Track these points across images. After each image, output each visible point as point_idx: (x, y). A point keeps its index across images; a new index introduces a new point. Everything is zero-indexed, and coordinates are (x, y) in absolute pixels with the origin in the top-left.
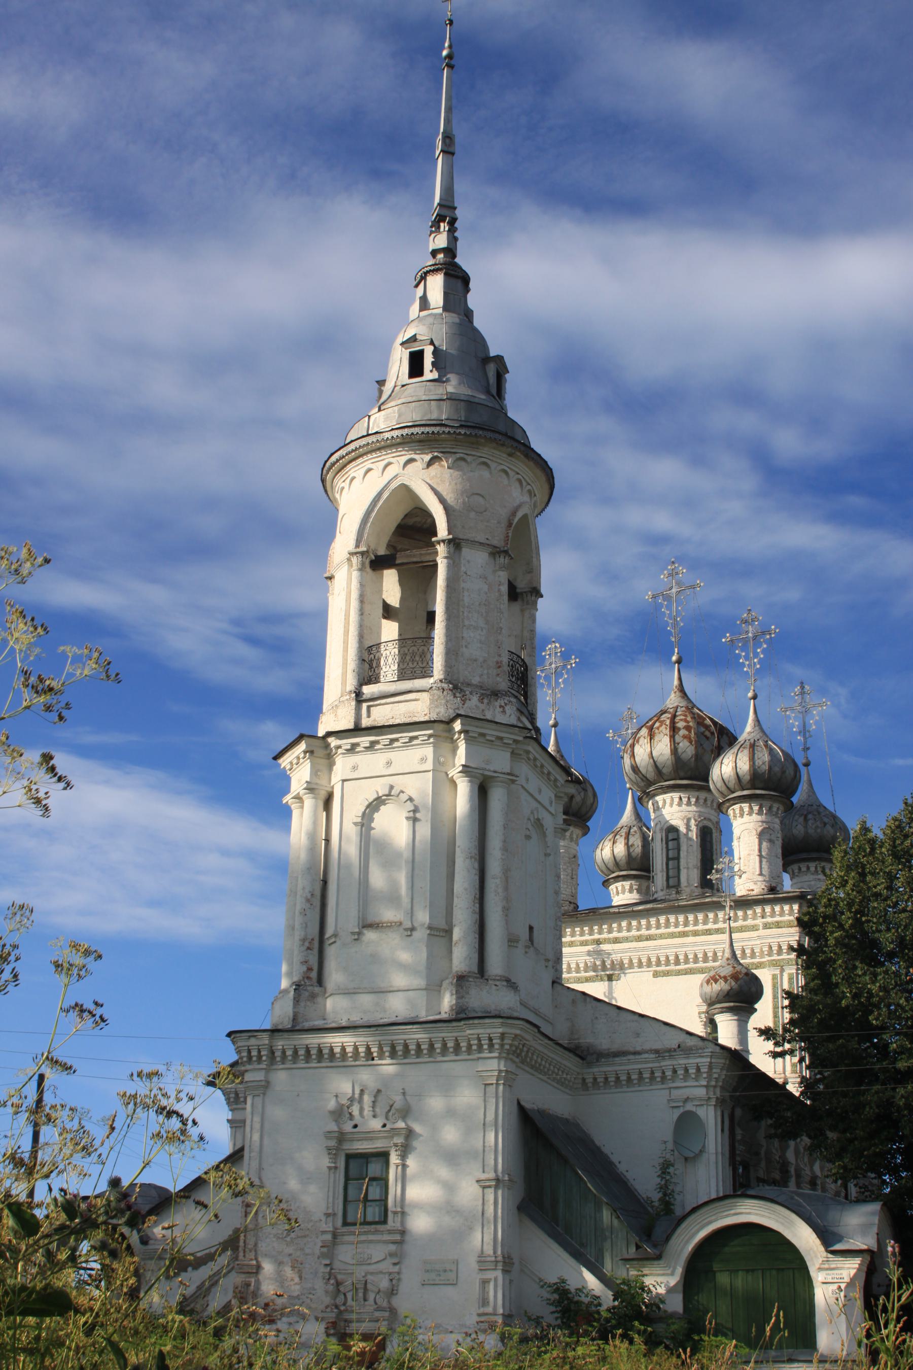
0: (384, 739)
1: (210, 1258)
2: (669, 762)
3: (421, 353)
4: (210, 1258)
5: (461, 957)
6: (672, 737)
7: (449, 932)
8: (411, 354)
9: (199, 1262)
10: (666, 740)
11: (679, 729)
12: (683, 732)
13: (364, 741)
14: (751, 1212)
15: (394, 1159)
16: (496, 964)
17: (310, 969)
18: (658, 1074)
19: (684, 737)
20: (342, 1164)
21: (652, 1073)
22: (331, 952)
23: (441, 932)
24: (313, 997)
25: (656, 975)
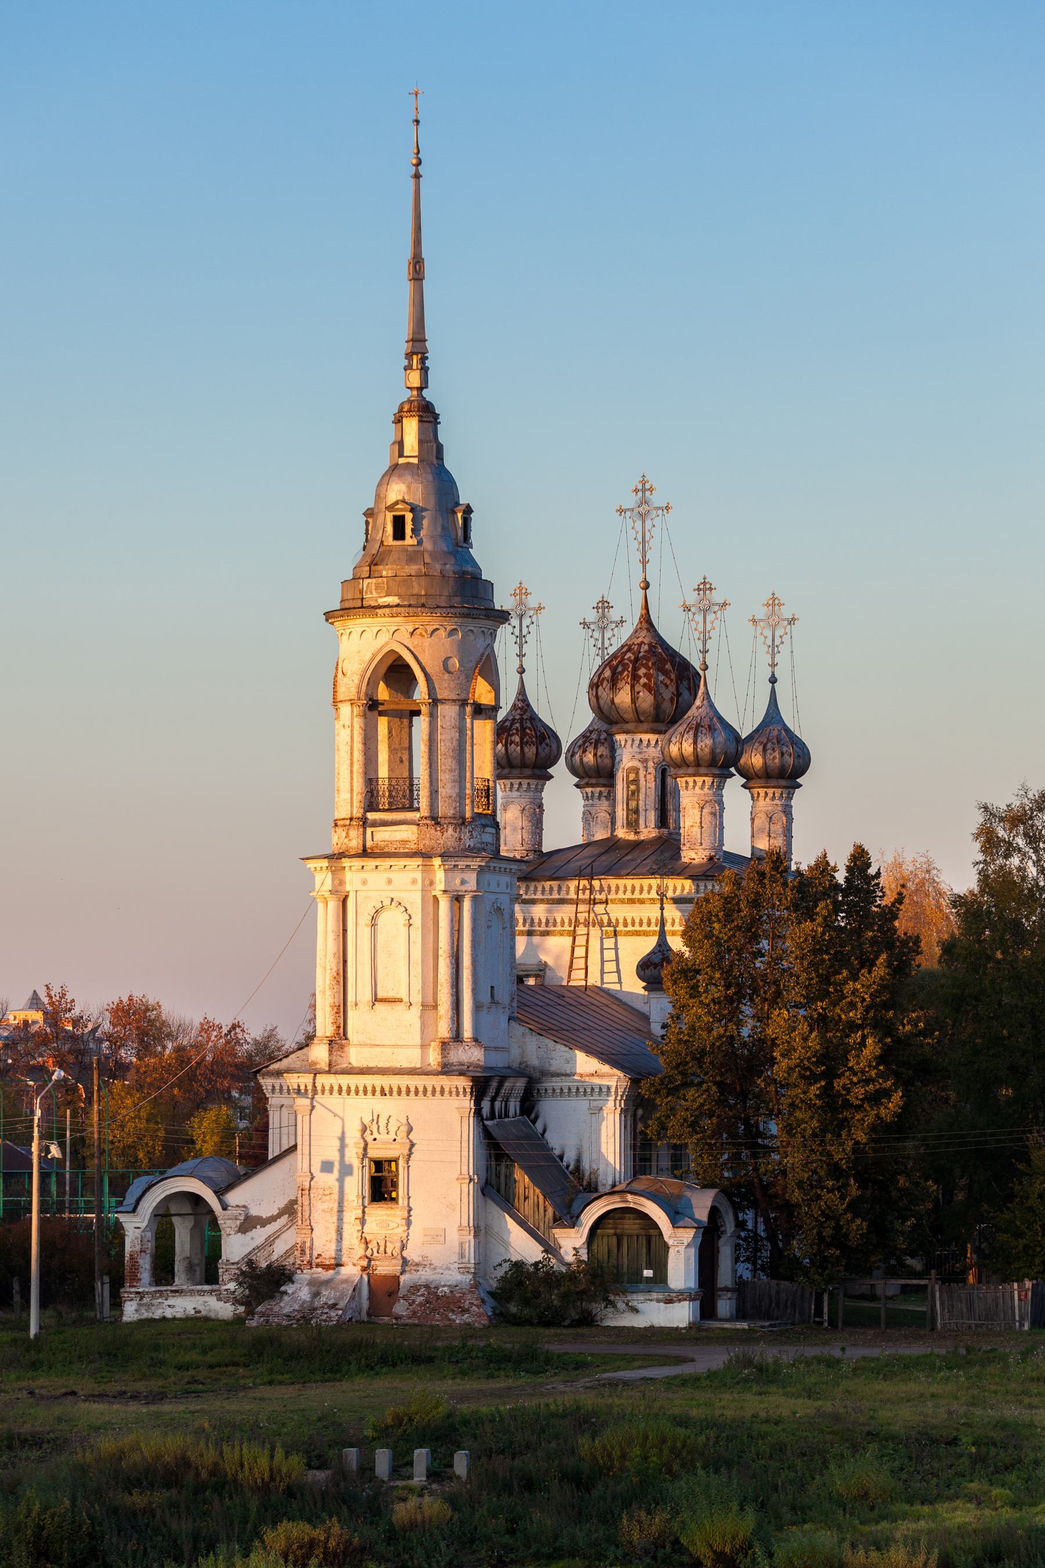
0: (388, 862)
1: (273, 1219)
2: (630, 710)
3: (403, 517)
4: (273, 1219)
5: (444, 1029)
6: (632, 687)
7: (435, 1007)
8: (395, 517)
9: (264, 1222)
10: (628, 687)
11: (640, 677)
12: (643, 680)
13: (370, 863)
14: (633, 1201)
15: (401, 1162)
16: (467, 1032)
17: (339, 1027)
18: (582, 1090)
19: (644, 685)
20: (366, 1162)
21: (578, 1089)
22: (351, 1013)
23: (429, 1006)
24: (342, 1047)
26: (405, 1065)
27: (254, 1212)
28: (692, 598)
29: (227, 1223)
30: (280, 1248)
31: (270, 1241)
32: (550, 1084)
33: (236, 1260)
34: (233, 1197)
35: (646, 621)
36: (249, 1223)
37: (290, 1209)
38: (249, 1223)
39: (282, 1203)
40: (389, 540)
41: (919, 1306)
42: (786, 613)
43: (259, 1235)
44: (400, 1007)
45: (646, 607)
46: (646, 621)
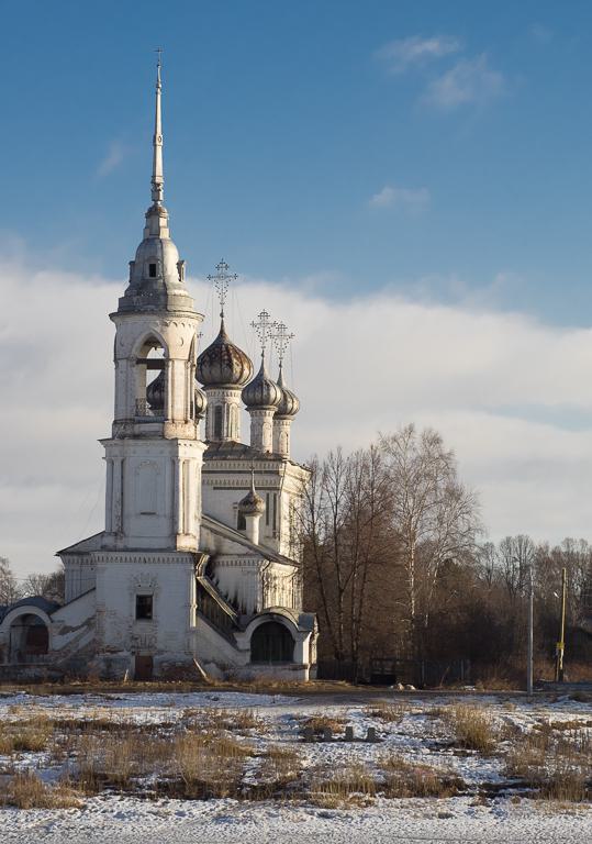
1: (79, 628)
4: (79, 628)
9: (74, 629)
25: (215, 488)
26: (156, 547)
27: (68, 624)
28: (257, 320)
29: (53, 632)
30: (83, 643)
31: (77, 639)
32: (222, 559)
33: (57, 648)
34: (57, 616)
35: (222, 332)
36: (65, 630)
37: (89, 623)
38: (65, 630)
39: (84, 619)
40: (148, 277)
41: (527, 641)
42: (288, 332)
43: (71, 636)
44: (154, 518)
45: (222, 326)
46: (222, 332)
